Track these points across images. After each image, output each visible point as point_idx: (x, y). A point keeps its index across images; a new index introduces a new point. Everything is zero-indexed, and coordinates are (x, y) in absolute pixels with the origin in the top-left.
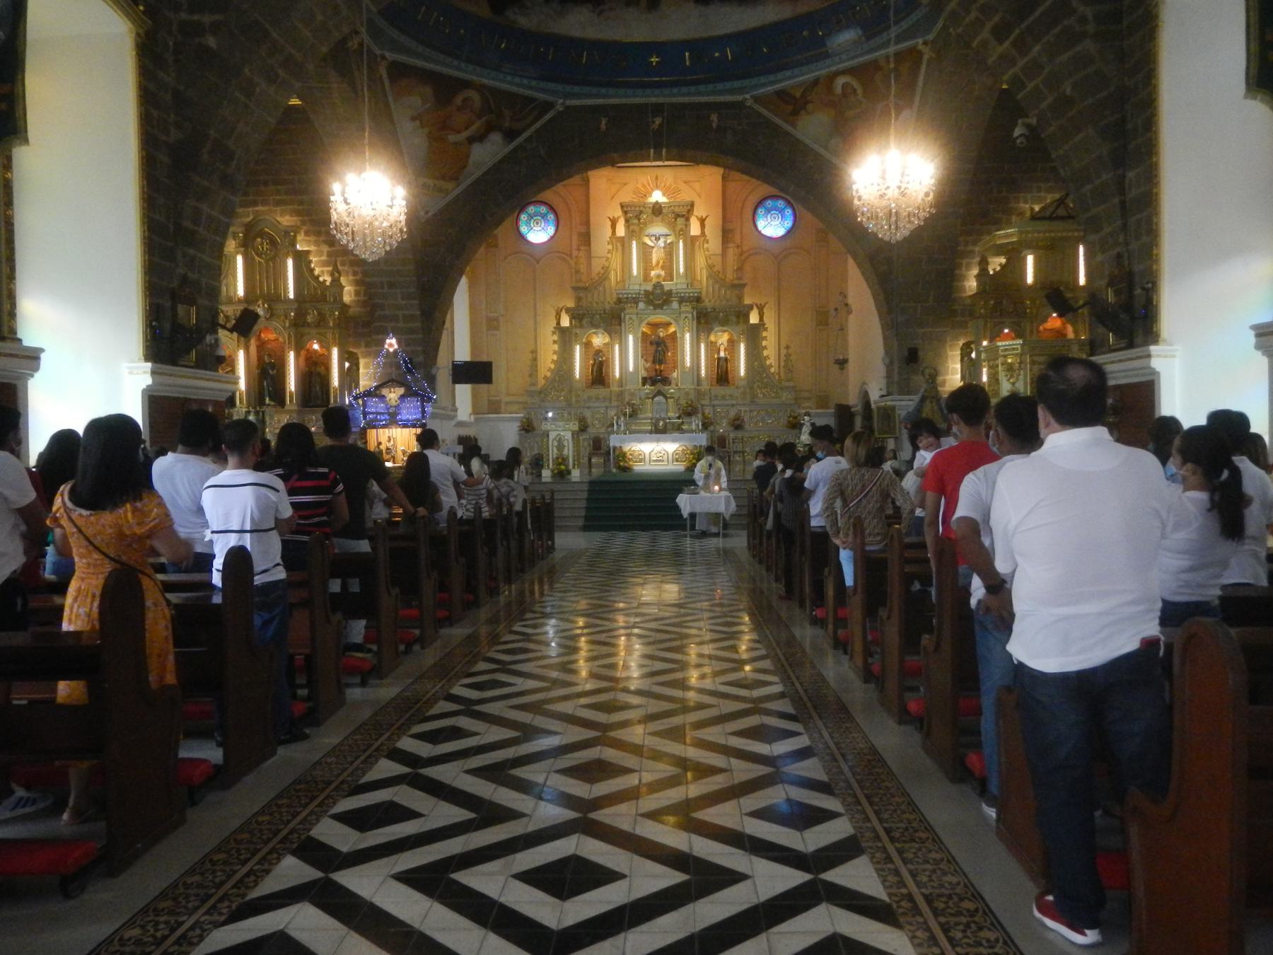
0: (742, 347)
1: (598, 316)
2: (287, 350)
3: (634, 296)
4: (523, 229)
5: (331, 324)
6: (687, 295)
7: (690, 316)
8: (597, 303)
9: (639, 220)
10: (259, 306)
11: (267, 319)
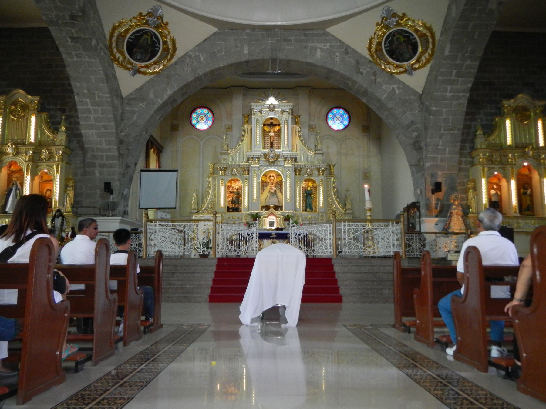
0: (321, 188)
1: (235, 170)
2: (25, 175)
3: (257, 156)
4: (194, 122)
5: (57, 159)
6: (289, 156)
7: (290, 169)
8: (235, 162)
9: (261, 113)
10: (9, 146)
11: (14, 155)
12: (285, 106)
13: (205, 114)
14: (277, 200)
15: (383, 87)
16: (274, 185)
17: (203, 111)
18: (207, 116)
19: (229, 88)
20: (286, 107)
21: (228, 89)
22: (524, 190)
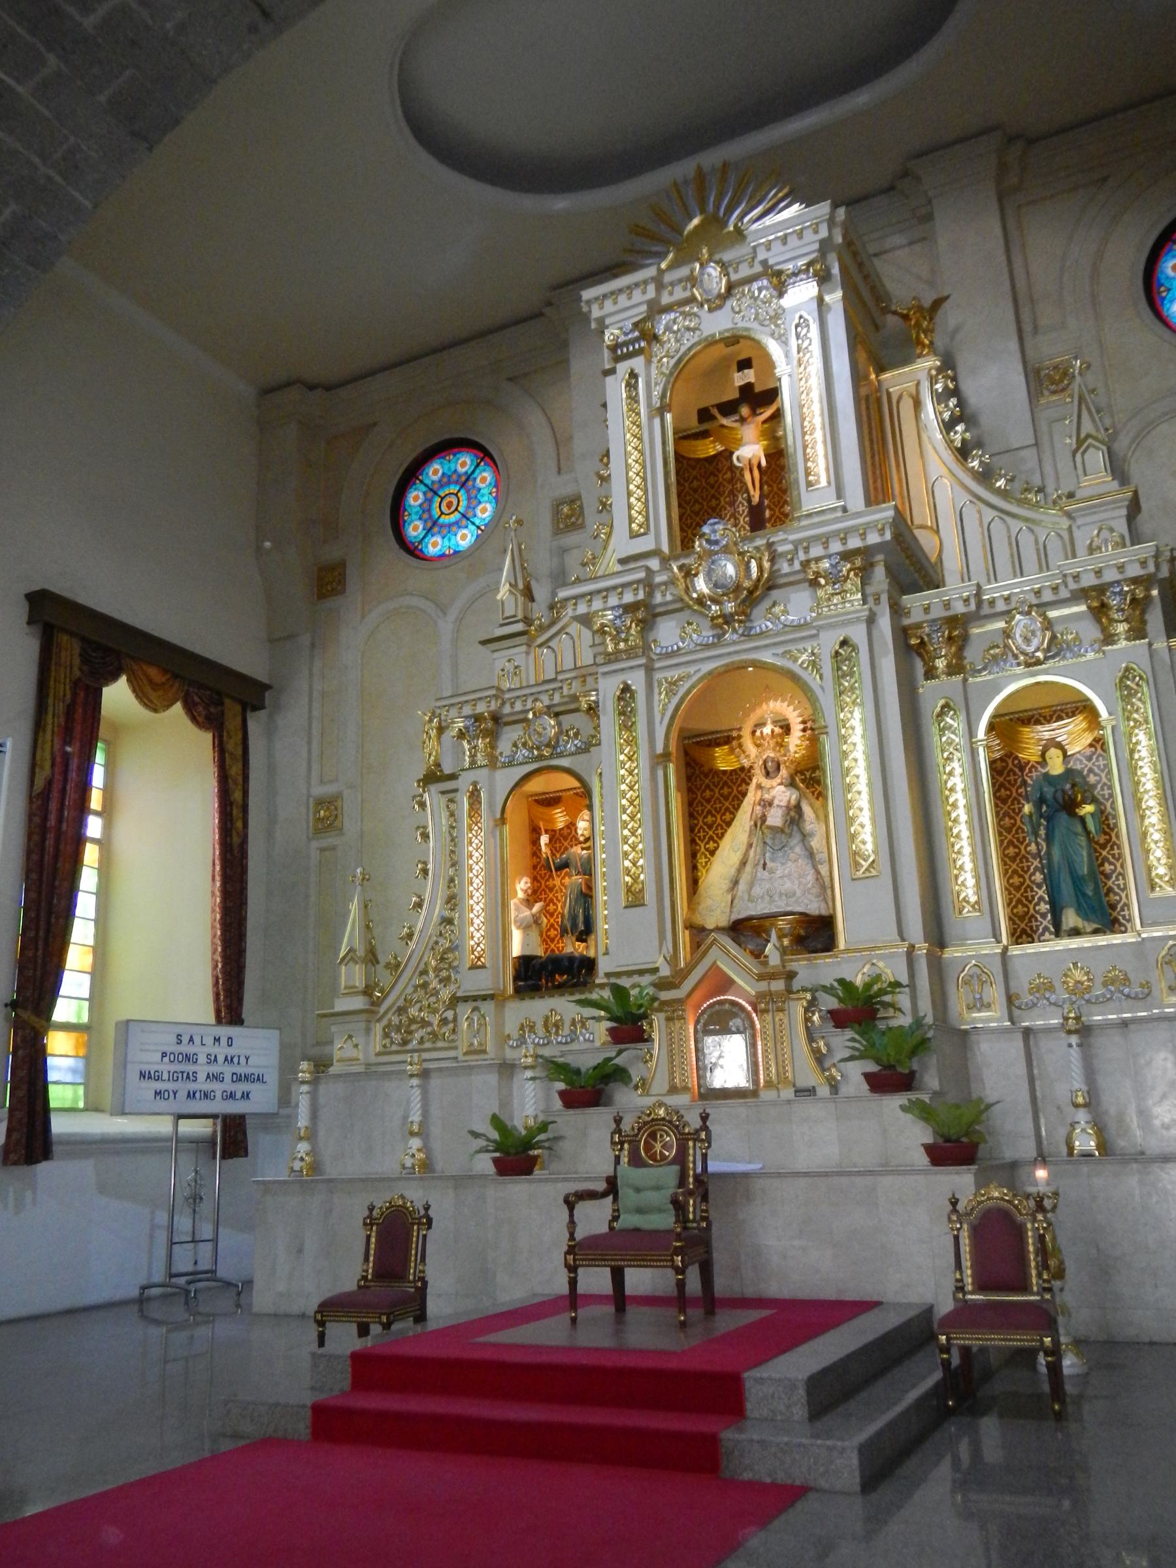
3: (629, 598)
4: (414, 530)
12: (784, 240)
13: (463, 478)
14: (810, 877)
16: (784, 772)
17: (453, 466)
18: (470, 483)
19: (549, 304)
20: (793, 241)
21: (547, 311)
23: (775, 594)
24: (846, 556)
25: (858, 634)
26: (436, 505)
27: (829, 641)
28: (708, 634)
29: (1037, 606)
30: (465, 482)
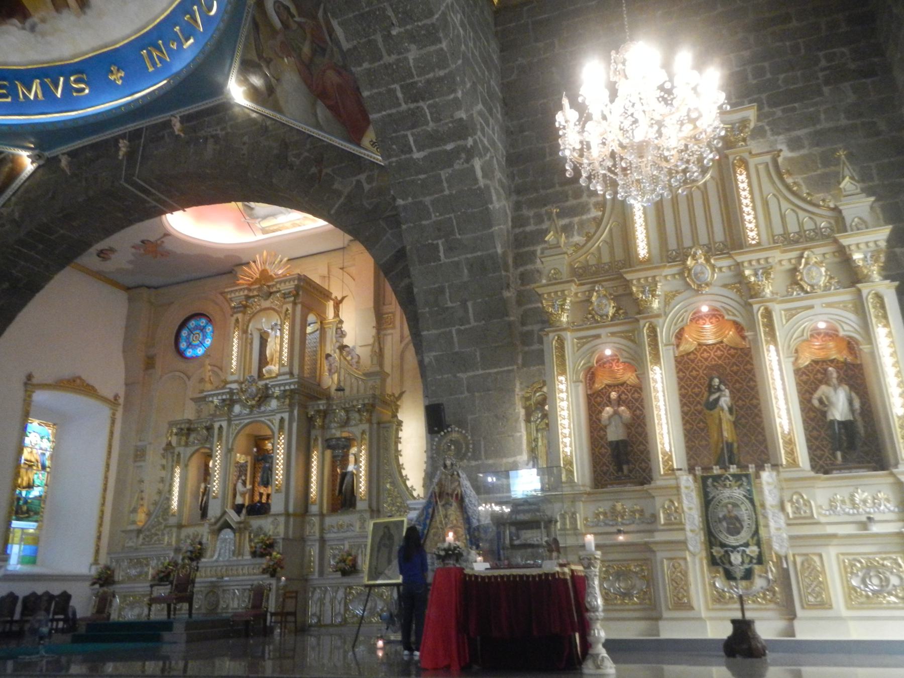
3: (224, 397)
4: (183, 345)
15: (336, 186)
22: (711, 393)
23: (268, 399)
24: (285, 391)
25: (286, 416)
26: (191, 337)
27: (278, 417)
28: (247, 411)
29: (344, 409)
30: (202, 329)
